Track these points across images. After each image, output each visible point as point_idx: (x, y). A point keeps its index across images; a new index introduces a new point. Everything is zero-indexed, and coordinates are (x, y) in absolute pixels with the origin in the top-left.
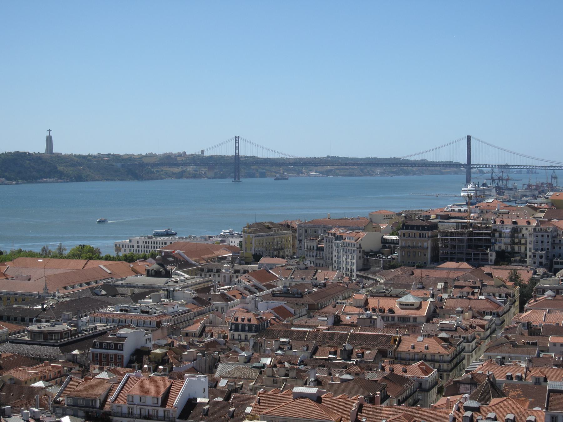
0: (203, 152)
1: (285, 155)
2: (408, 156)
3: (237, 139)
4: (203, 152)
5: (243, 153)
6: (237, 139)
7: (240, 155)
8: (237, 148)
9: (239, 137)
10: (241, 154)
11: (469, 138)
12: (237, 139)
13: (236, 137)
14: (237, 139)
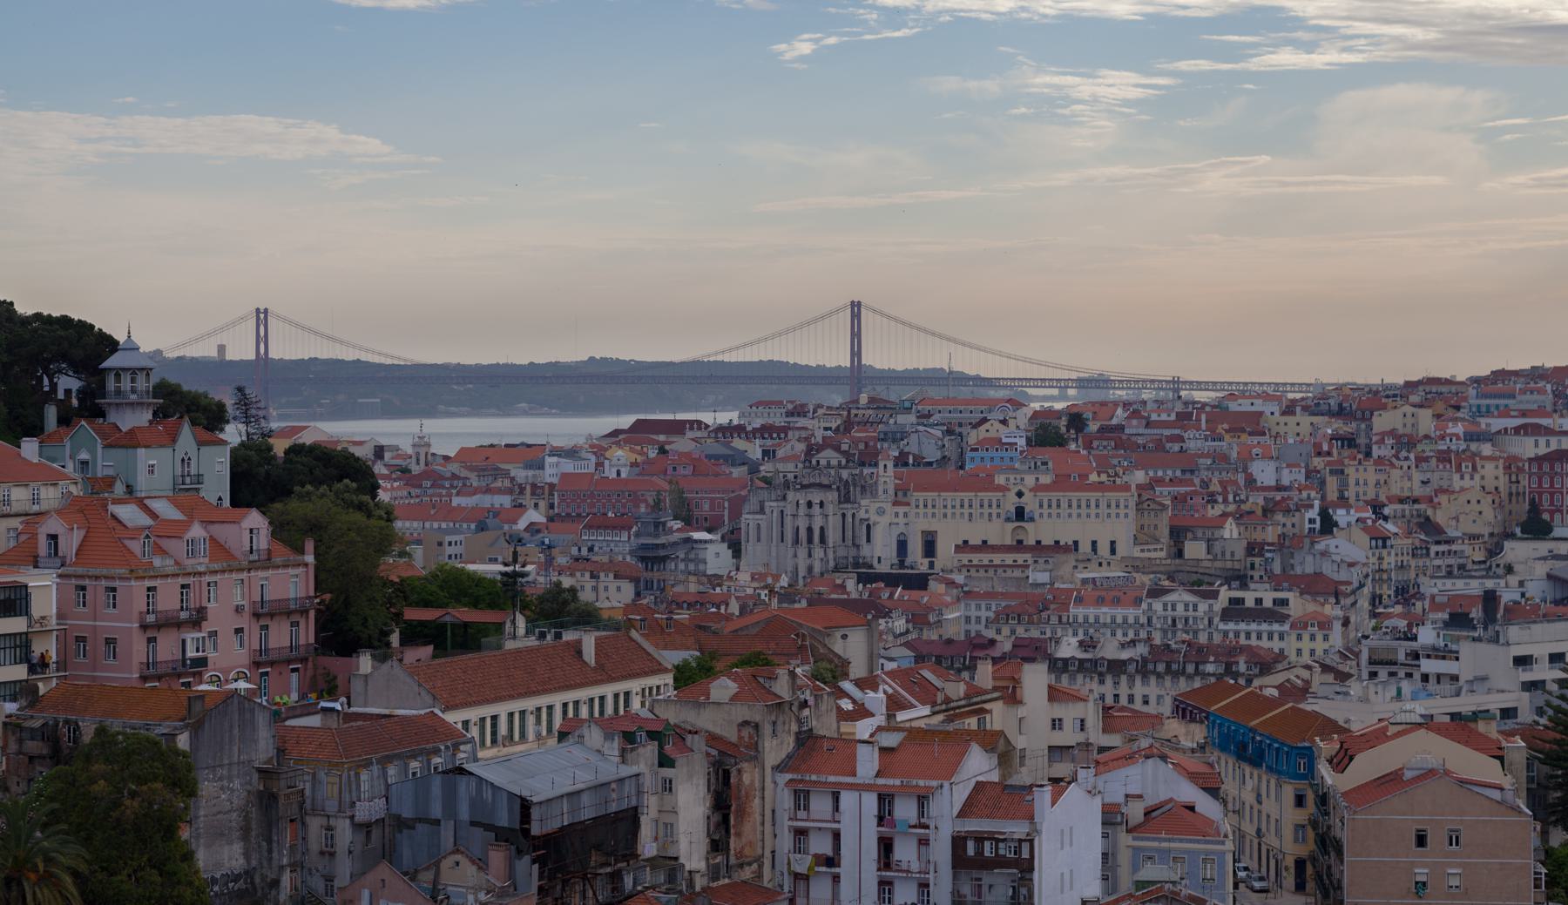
0: (221, 348)
1: (386, 356)
2: (717, 353)
3: (262, 317)
4: (221, 348)
5: (274, 354)
6: (262, 316)
7: (270, 356)
8: (262, 339)
9: (266, 311)
10: (272, 355)
11: (856, 308)
12: (262, 316)
13: (258, 310)
14: (262, 316)
